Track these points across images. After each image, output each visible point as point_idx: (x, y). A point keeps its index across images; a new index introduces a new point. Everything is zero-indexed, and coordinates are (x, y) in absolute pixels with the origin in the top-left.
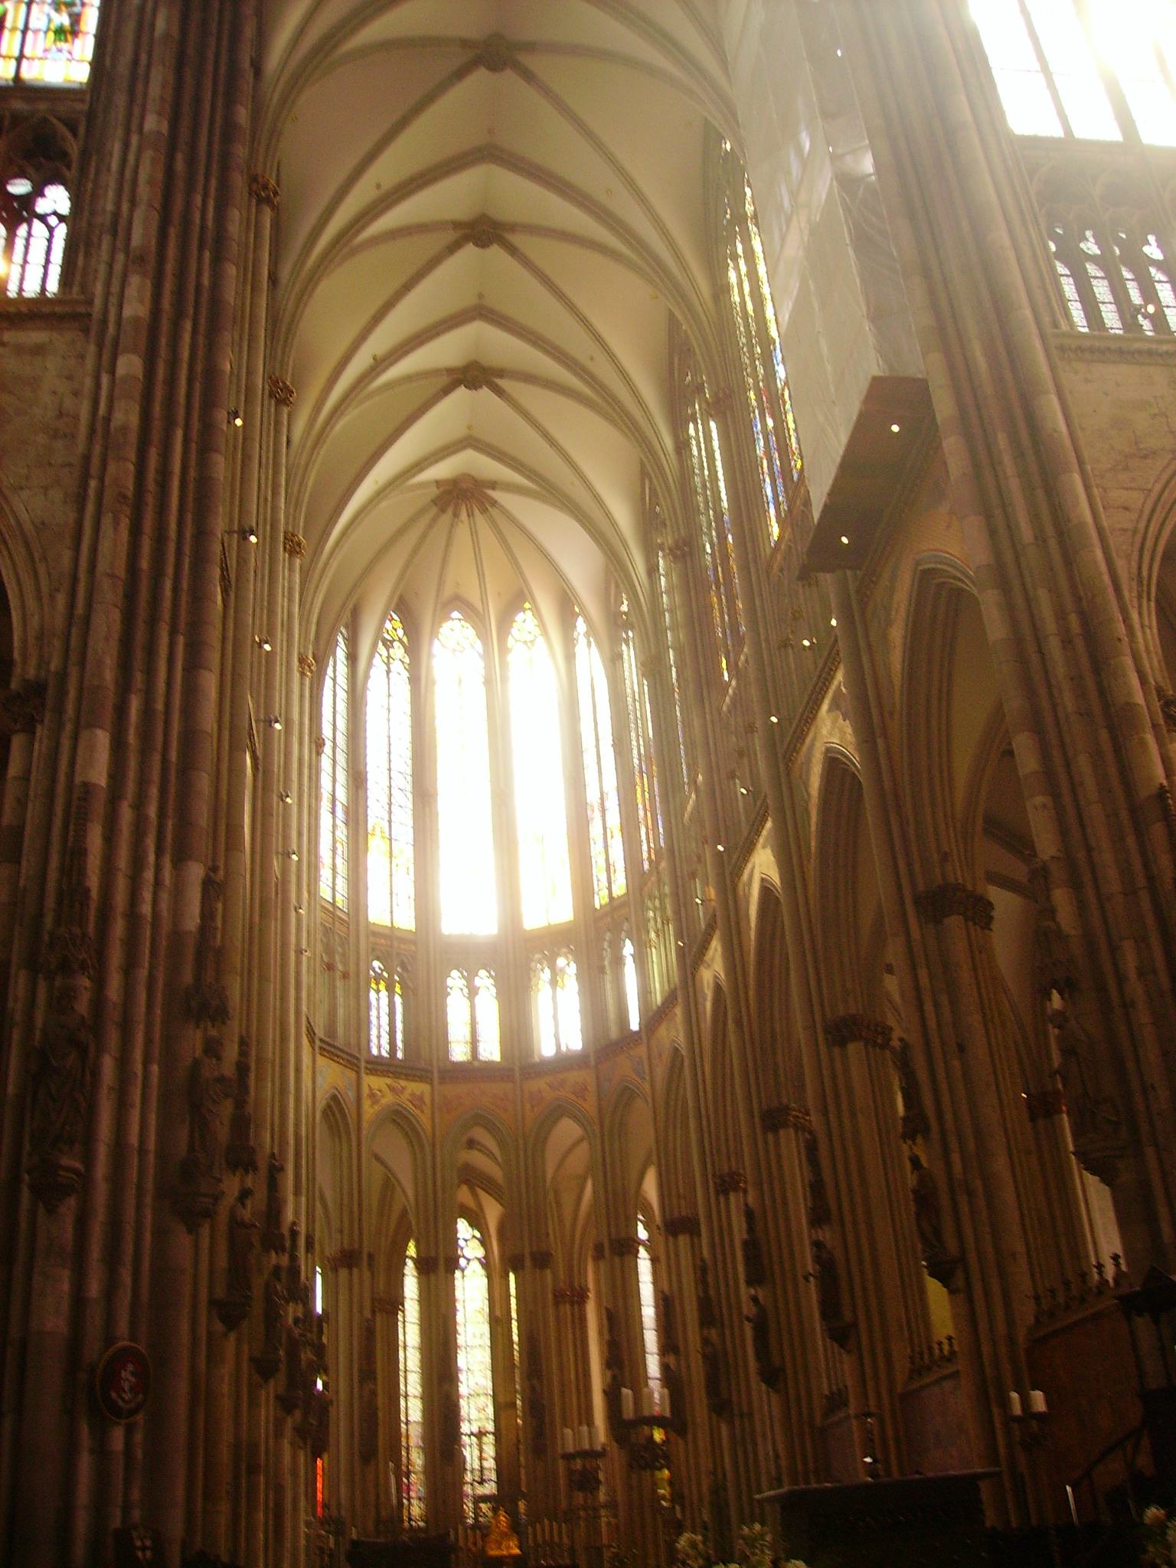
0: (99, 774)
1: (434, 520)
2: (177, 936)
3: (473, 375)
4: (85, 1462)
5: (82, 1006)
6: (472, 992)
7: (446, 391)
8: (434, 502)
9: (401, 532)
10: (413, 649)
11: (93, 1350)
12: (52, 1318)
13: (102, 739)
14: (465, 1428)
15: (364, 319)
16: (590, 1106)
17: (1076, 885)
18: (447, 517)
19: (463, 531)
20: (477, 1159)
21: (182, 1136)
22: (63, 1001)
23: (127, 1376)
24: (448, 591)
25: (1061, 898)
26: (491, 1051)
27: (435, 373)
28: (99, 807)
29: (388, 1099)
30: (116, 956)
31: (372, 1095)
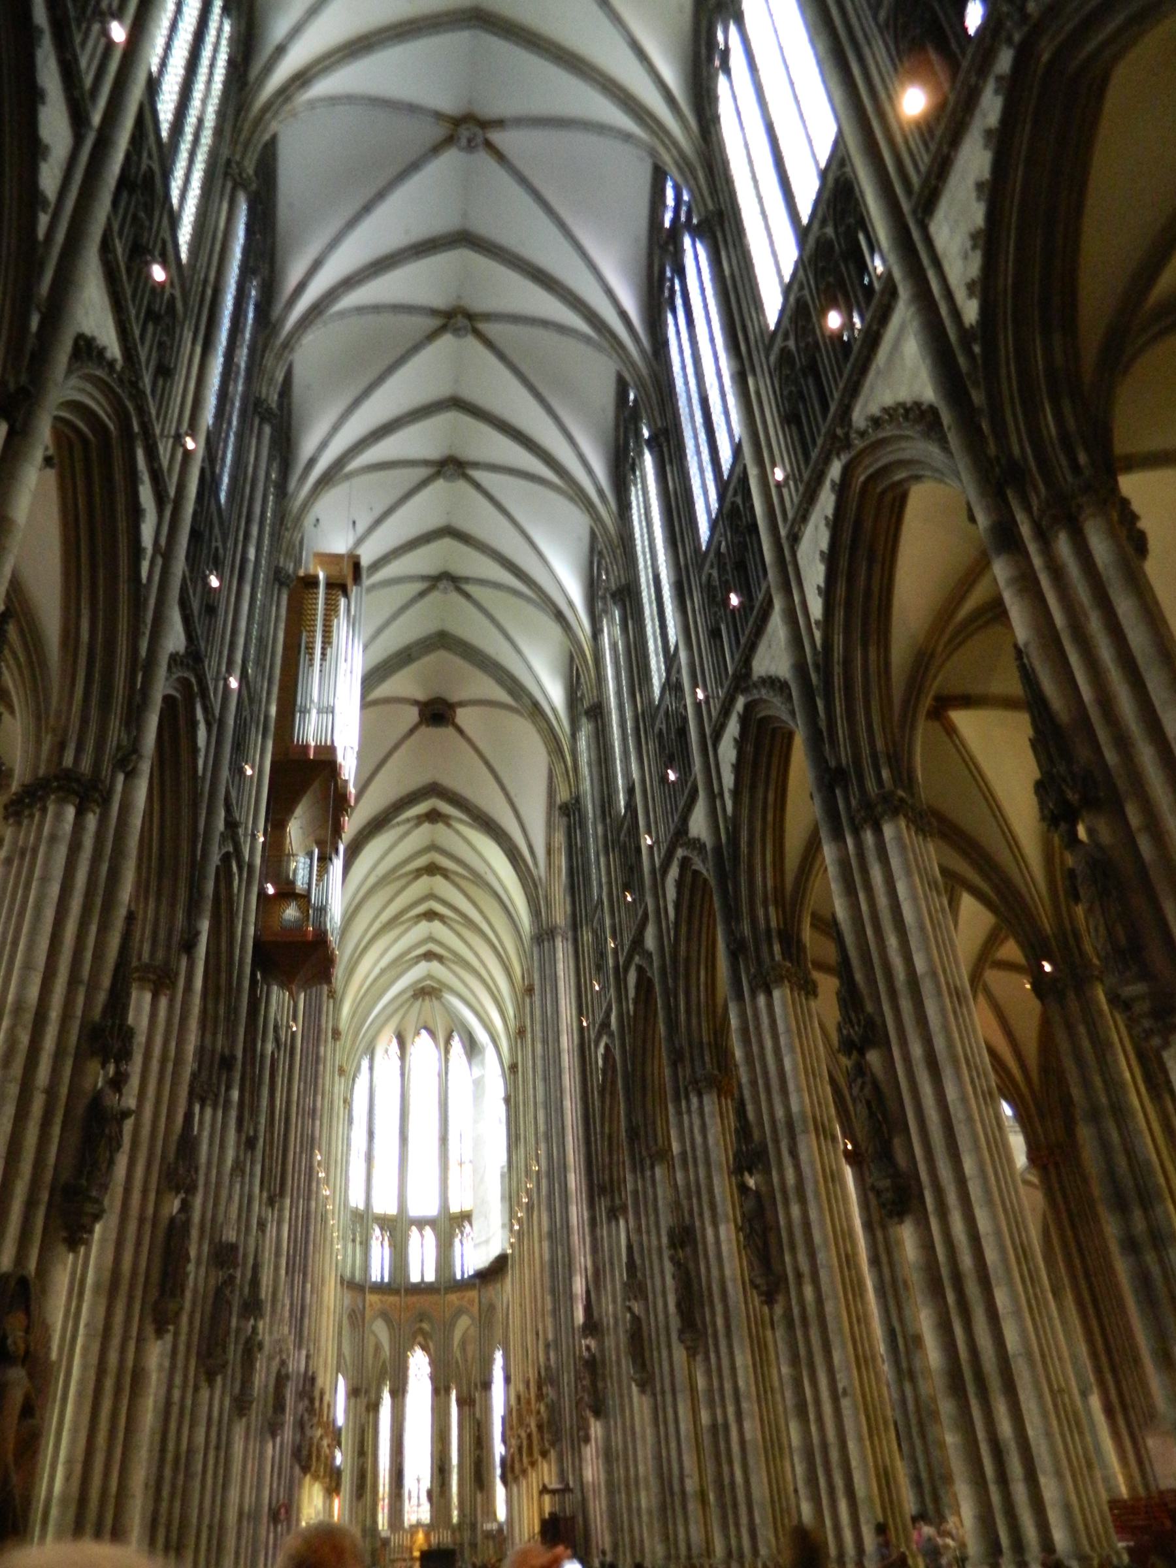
1: (411, 1005)
2: (298, 1374)
3: (429, 956)
4: (271, 1536)
7: (417, 963)
9: (396, 1011)
10: (403, 1057)
11: (274, 1502)
16: (475, 1310)
17: (556, 1349)
18: (418, 1004)
19: (427, 1001)
20: (426, 1326)
21: (298, 1437)
23: (283, 1511)
25: (552, 1354)
29: (379, 1305)
31: (371, 1305)
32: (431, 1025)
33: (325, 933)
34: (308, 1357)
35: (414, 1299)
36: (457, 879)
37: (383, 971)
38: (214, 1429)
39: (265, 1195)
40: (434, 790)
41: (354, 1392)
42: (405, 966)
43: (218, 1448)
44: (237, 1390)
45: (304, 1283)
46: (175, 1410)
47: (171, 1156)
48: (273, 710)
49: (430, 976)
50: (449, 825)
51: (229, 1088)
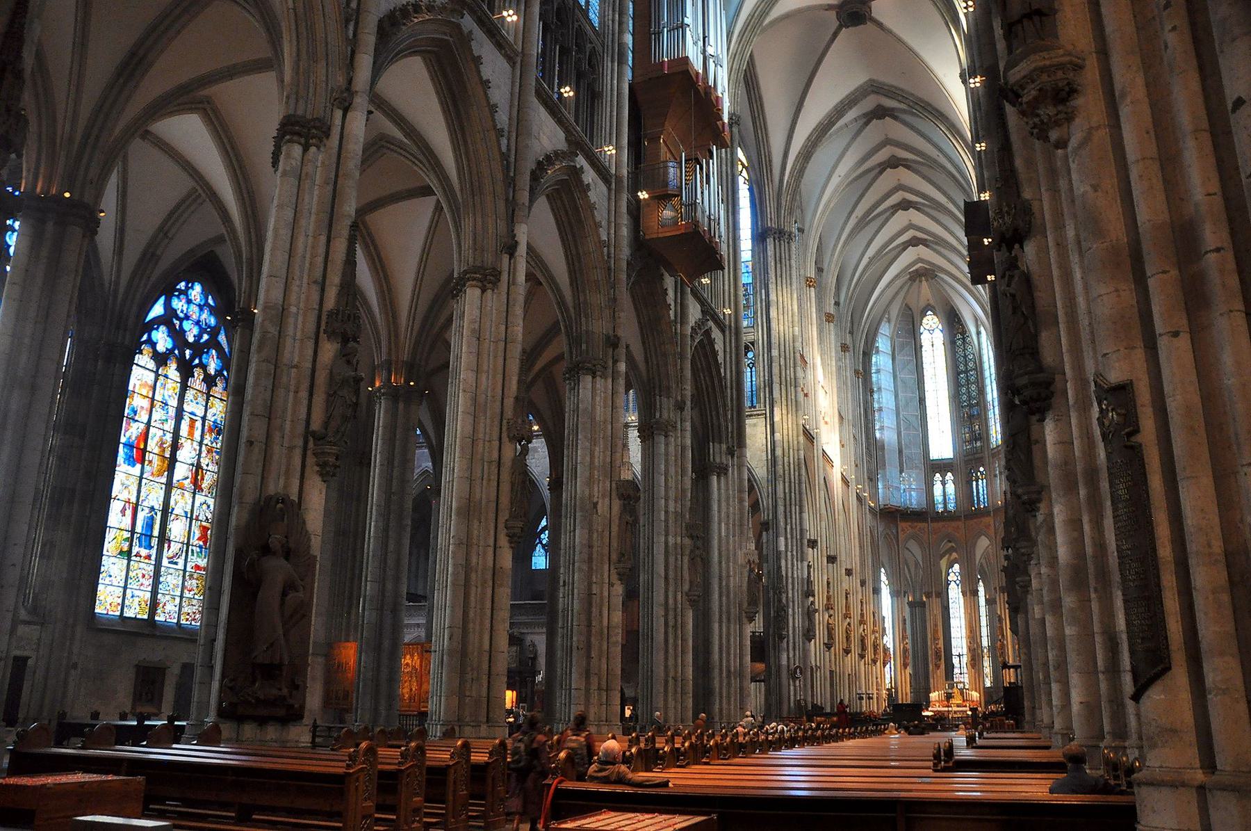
0: (782, 548)
5: (784, 600)
6: (944, 483)
7: (904, 249)
8: (910, 279)
9: (897, 293)
12: (784, 662)
13: (782, 539)
14: (954, 652)
15: (862, 249)
19: (924, 283)
22: (780, 601)
24: (922, 304)
26: (951, 506)
27: (897, 246)
28: (783, 556)
30: (790, 587)
32: (932, 302)
33: (696, 223)
34: (809, 567)
35: (940, 524)
36: (920, 168)
37: (871, 259)
38: (671, 613)
39: (724, 446)
40: (873, 88)
41: (895, 594)
42: (894, 253)
43: (675, 626)
44: (686, 587)
45: (801, 512)
46: (596, 600)
47: (509, 413)
48: (629, 39)
49: (920, 260)
50: (895, 118)
51: (615, 362)
